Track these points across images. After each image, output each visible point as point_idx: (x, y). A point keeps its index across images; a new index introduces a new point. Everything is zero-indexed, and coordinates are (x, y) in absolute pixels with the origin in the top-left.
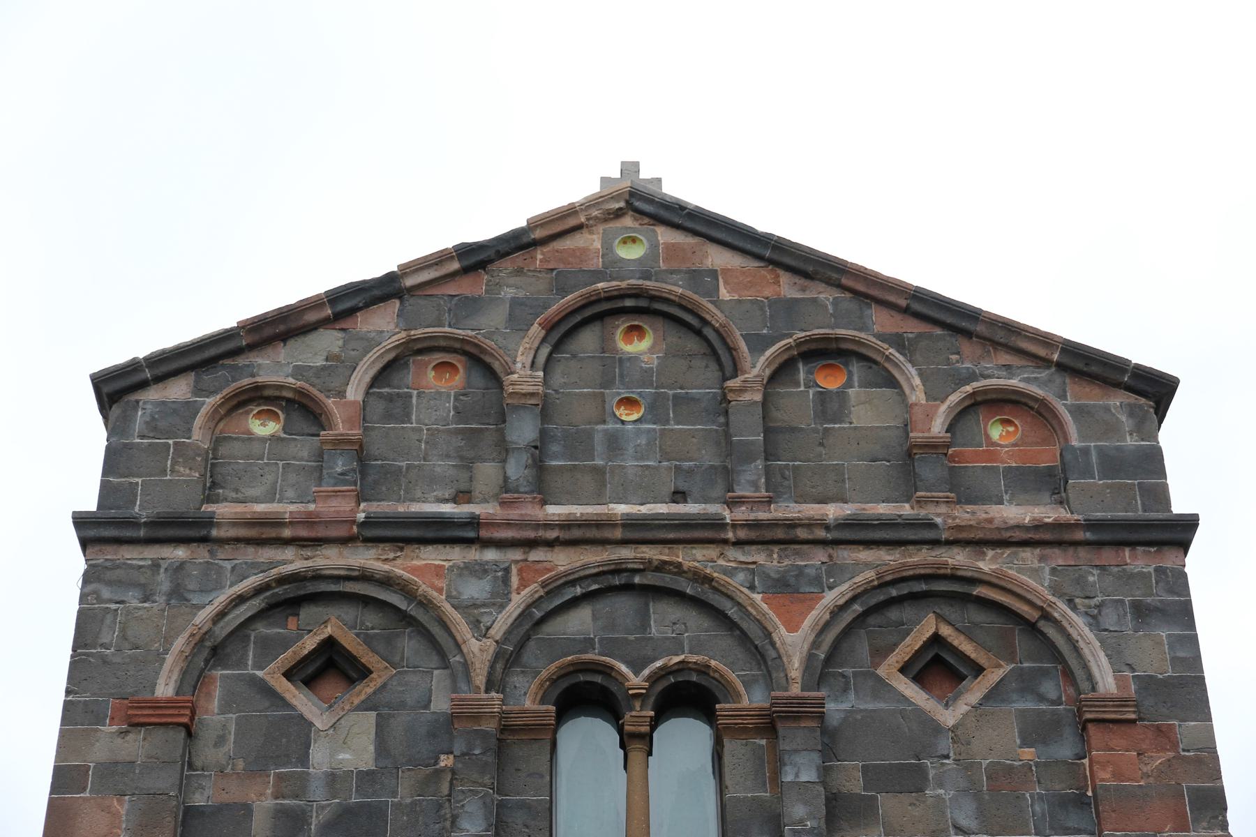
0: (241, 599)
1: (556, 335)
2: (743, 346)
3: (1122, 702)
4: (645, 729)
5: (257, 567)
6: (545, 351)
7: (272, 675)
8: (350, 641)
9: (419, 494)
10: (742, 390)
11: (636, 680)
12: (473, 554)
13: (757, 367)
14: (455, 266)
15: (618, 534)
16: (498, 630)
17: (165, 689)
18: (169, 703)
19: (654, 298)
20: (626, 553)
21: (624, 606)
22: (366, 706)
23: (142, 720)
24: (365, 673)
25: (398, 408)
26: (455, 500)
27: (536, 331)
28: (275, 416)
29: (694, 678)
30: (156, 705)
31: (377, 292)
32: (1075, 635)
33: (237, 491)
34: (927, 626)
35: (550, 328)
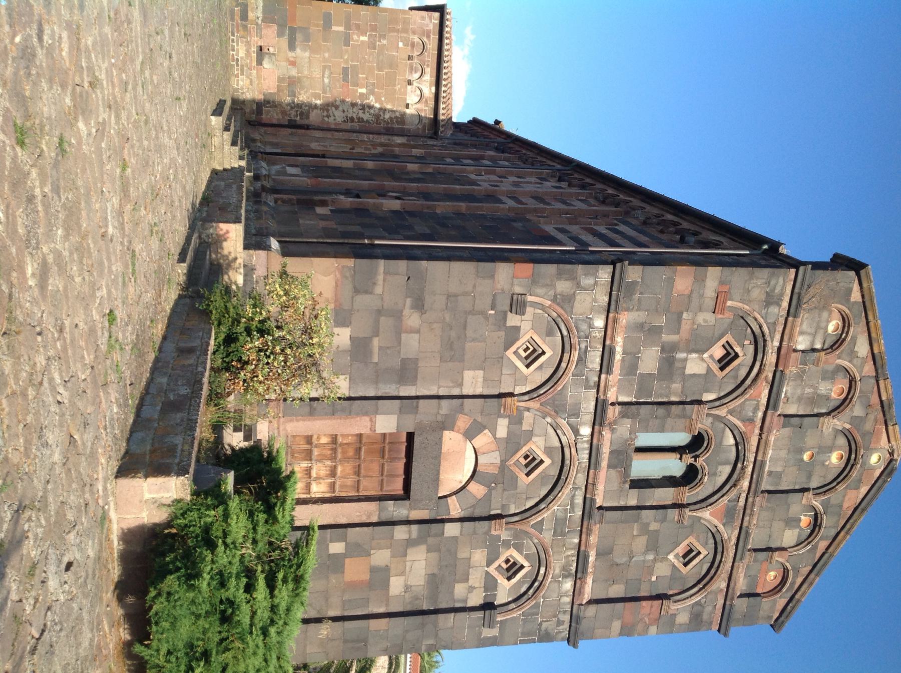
0: (761, 327)
3: (667, 612)
7: (728, 337)
12: (763, 408)
13: (817, 503)
14: (884, 398)
15: (759, 458)
16: (730, 417)
19: (853, 466)
20: (751, 457)
22: (709, 370)
23: (718, 301)
24: (722, 369)
27: (848, 426)
29: (699, 477)
30: (725, 302)
32: (693, 598)
34: (704, 552)
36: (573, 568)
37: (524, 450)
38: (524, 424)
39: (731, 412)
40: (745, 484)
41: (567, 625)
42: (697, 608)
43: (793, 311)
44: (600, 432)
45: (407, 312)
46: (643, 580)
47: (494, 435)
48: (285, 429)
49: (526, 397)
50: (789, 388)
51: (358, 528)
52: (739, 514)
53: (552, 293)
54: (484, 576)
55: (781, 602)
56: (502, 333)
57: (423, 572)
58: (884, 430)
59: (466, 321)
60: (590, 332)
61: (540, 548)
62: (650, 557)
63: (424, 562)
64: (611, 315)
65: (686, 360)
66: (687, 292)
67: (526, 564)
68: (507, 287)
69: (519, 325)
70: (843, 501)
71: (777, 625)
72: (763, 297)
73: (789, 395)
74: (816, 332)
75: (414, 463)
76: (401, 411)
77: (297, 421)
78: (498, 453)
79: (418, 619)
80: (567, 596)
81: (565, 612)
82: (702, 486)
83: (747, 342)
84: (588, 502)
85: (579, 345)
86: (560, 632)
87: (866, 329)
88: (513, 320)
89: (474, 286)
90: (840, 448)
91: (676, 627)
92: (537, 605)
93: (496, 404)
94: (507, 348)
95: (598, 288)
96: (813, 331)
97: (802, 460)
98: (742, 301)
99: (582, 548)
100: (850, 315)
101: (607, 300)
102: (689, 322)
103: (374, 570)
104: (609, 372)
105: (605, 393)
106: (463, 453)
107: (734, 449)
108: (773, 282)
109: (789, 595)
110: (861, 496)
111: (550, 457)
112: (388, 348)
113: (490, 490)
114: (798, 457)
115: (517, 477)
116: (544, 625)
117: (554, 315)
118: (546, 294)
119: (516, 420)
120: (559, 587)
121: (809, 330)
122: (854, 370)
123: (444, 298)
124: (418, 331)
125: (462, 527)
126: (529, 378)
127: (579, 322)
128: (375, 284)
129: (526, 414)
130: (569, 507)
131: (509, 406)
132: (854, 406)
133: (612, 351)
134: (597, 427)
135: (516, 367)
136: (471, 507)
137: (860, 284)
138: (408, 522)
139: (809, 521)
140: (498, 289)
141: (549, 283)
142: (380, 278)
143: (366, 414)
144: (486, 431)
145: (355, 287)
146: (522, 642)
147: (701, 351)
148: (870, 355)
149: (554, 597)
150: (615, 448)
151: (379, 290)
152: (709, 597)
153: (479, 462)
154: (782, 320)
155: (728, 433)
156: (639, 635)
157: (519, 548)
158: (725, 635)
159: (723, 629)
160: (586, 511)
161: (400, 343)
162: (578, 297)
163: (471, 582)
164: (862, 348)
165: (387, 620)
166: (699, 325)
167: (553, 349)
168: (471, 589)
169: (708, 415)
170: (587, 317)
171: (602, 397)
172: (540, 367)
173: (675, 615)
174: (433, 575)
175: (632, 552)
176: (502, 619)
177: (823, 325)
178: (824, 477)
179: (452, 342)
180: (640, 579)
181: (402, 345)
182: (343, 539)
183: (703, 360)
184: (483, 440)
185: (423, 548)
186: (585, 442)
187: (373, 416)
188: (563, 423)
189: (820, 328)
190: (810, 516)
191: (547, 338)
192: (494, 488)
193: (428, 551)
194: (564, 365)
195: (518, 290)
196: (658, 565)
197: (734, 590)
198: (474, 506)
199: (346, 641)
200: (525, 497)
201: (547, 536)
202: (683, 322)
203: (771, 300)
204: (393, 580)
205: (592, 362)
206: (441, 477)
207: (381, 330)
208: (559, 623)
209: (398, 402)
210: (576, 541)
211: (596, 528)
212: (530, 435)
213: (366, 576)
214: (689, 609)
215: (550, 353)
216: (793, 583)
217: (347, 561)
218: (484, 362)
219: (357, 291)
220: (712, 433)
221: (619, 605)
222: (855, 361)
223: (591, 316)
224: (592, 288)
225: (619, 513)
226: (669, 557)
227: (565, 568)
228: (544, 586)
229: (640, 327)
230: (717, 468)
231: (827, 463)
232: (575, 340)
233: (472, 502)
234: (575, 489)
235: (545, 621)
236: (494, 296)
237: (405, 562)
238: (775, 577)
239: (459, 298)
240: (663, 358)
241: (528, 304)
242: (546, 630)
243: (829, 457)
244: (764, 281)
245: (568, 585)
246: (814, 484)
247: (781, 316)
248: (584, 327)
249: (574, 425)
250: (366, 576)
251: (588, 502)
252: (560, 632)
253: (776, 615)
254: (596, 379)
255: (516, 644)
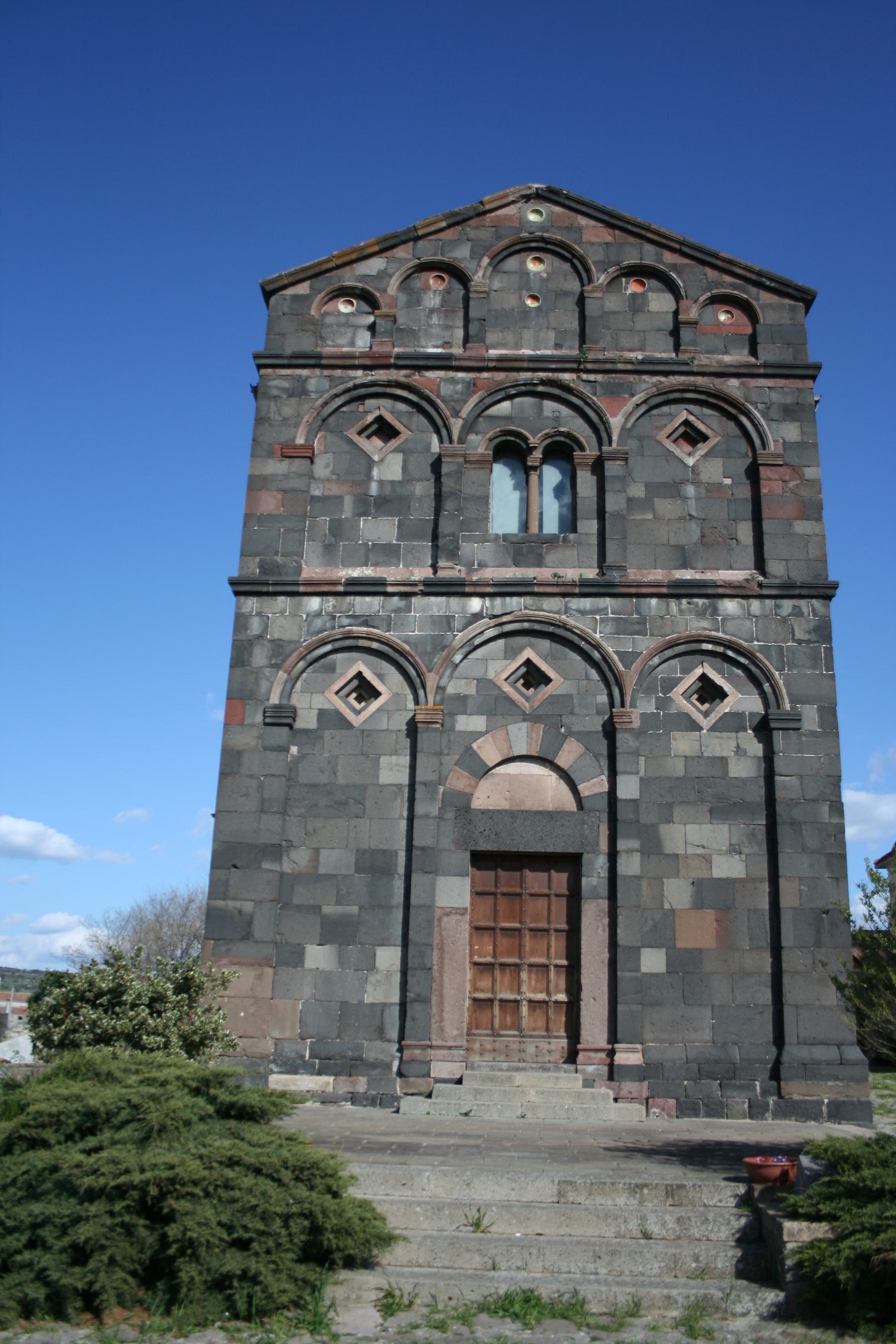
0: (337, 396)
1: (496, 261)
2: (593, 268)
3: (778, 456)
4: (537, 464)
5: (343, 380)
6: (490, 269)
8: (389, 418)
9: (423, 342)
10: (593, 291)
11: (533, 441)
12: (451, 374)
13: (602, 279)
14: (444, 224)
16: (464, 413)
17: (300, 440)
18: (302, 447)
21: (528, 400)
22: (397, 450)
25: (415, 300)
26: (442, 346)
27: (486, 260)
28: (352, 303)
29: (562, 439)
30: (296, 447)
31: (403, 238)
33: (333, 341)
34: (684, 415)
35: (492, 259)
36: (700, 602)
37: (507, 688)
38: (466, 693)
39: (456, 414)
40: (566, 377)
41: (802, 603)
42: (774, 413)
43: (314, 361)
44: (475, 584)
45: (287, 867)
46: (730, 497)
47: (481, 734)
48: (454, 1039)
49: (421, 693)
50: (430, 344)
51: (619, 931)
52: (614, 378)
53: (267, 672)
54: (718, 734)
55: (766, 297)
56: (327, 734)
57: (707, 828)
58: (493, 214)
59: (306, 785)
60: (328, 614)
61: (669, 653)
62: (690, 490)
63: (688, 826)
64: (302, 589)
65: (381, 483)
66: (279, 496)
67: (698, 671)
68: (255, 733)
69: (316, 712)
70: (600, 244)
71: (806, 298)
72: (294, 400)
73: (439, 343)
74: (352, 326)
75: (521, 850)
76: (434, 871)
77: (442, 1020)
78: (510, 727)
79: (784, 834)
80: (749, 606)
81: (777, 606)
82: (575, 434)
83: (361, 409)
84: (587, 589)
85: (344, 626)
86: (814, 610)
87: (348, 268)
88: (307, 720)
89: (251, 776)
90: (523, 263)
91: (805, 440)
92: (764, 650)
93: (425, 735)
94: (348, 725)
95: (266, 610)
96: (350, 330)
97: (538, 309)
98: (297, 426)
99: (664, 590)
100: (328, 290)
101: (281, 599)
102: (328, 486)
103: (699, 903)
104: (382, 583)
105: (414, 584)
106: (512, 778)
107: (517, 400)
108: (275, 392)
109: (753, 290)
110: (592, 223)
111: (521, 650)
112: (338, 892)
113: (570, 734)
114: (533, 314)
115: (551, 696)
116: (799, 635)
117: (301, 665)
118: (268, 679)
119: (461, 703)
120: (733, 618)
121: (349, 335)
122: (403, 269)
123: (265, 817)
124: (317, 851)
125: (625, 773)
126: (395, 691)
127: (312, 630)
128: (240, 912)
129: (450, 690)
130: (598, 617)
131: (429, 716)
132: (455, 259)
133: (351, 582)
134: (467, 589)
135: (379, 710)
136: (598, 761)
137: (285, 287)
138: (613, 856)
139: (635, 283)
140: (258, 744)
141: (254, 676)
142: (231, 904)
143: (430, 922)
144: (475, 746)
145: (242, 939)
146: (830, 666)
147: (370, 463)
148: (384, 255)
149: (750, 626)
150: (510, 561)
151: (248, 907)
152: (754, 398)
153: (524, 752)
154: (326, 372)
155: (494, 410)
156: (820, 492)
157: (670, 684)
158: (818, 367)
159: (811, 372)
160: (602, 590)
161: (332, 876)
162: (276, 636)
163: (725, 754)
164: (375, 265)
165: (782, 882)
166: (333, 473)
167: (355, 661)
168: (739, 751)
169: (461, 441)
170: (306, 620)
171: (422, 588)
172: (381, 677)
173: (785, 443)
174: (711, 811)
175: (680, 519)
176: (787, 700)
177: (343, 319)
178: (565, 276)
179: (336, 802)
180: (729, 501)
181: (335, 872)
182: (635, 952)
183: (382, 461)
184: (489, 751)
185: (664, 829)
186: (492, 606)
187: (438, 913)
188: (460, 637)
189: (347, 322)
190: (627, 283)
191: (338, 670)
192: (568, 729)
193: (670, 820)
194: (375, 645)
195: (259, 718)
196: (704, 477)
197: (740, 366)
198: (596, 756)
199: (818, 944)
200: (585, 682)
201: (645, 644)
202: (328, 493)
203: (299, 391)
204: (717, 873)
205: (370, 606)
206: (550, 807)
207: (311, 902)
208: (797, 612)
209: (415, 878)
210: (654, 601)
211: (633, 574)
212: (484, 683)
213: (710, 915)
214: (774, 424)
215: (362, 665)
216: (733, 286)
217: (680, 944)
218: (367, 756)
219: (247, 936)
220: (491, 433)
221: (767, 526)
222: (390, 271)
223: (304, 616)
224: (265, 618)
225: (609, 544)
226: (691, 464)
227: (701, 614)
228: (729, 641)
229: (329, 550)
230: (548, 418)
231: (545, 275)
232: (338, 632)
233: (589, 760)
234: (567, 610)
235: (793, 635)
236: (266, 749)
237: (686, 856)
238: (728, 312)
239: (266, 796)
240: (376, 512)
241: (285, 702)
242: (809, 632)
243: (536, 274)
244: (272, 404)
245: (730, 606)
246: (574, 285)
247: (322, 373)
248: (318, 623)
249: (464, 621)
250: (710, 915)
251: (586, 590)
252: (814, 610)
253: (787, 301)
254: (396, 599)
255: (833, 676)
